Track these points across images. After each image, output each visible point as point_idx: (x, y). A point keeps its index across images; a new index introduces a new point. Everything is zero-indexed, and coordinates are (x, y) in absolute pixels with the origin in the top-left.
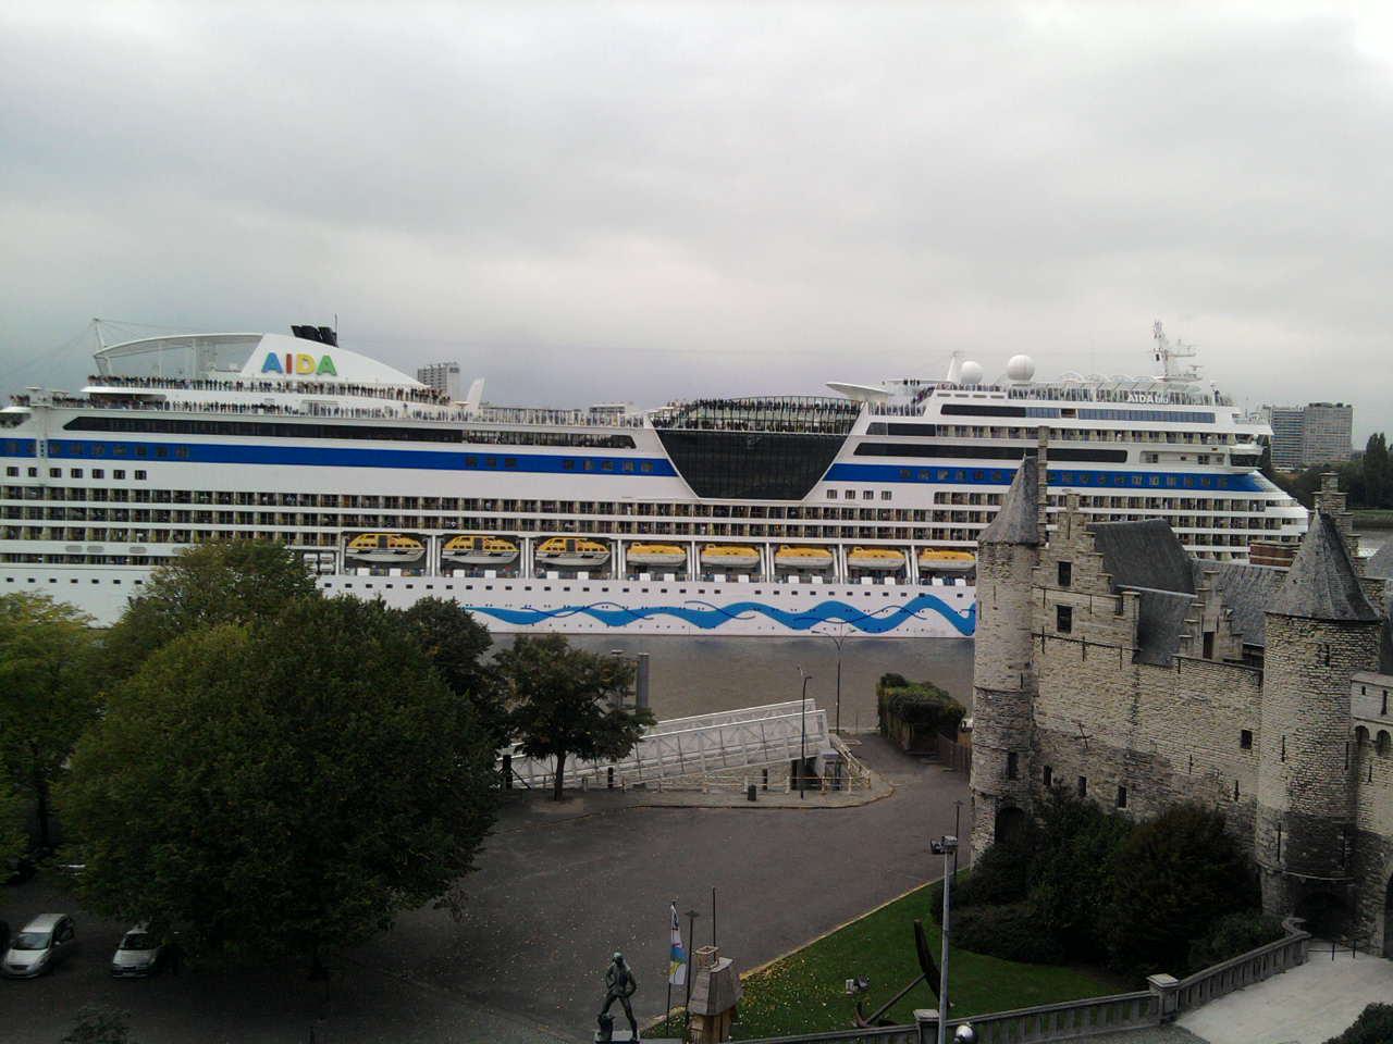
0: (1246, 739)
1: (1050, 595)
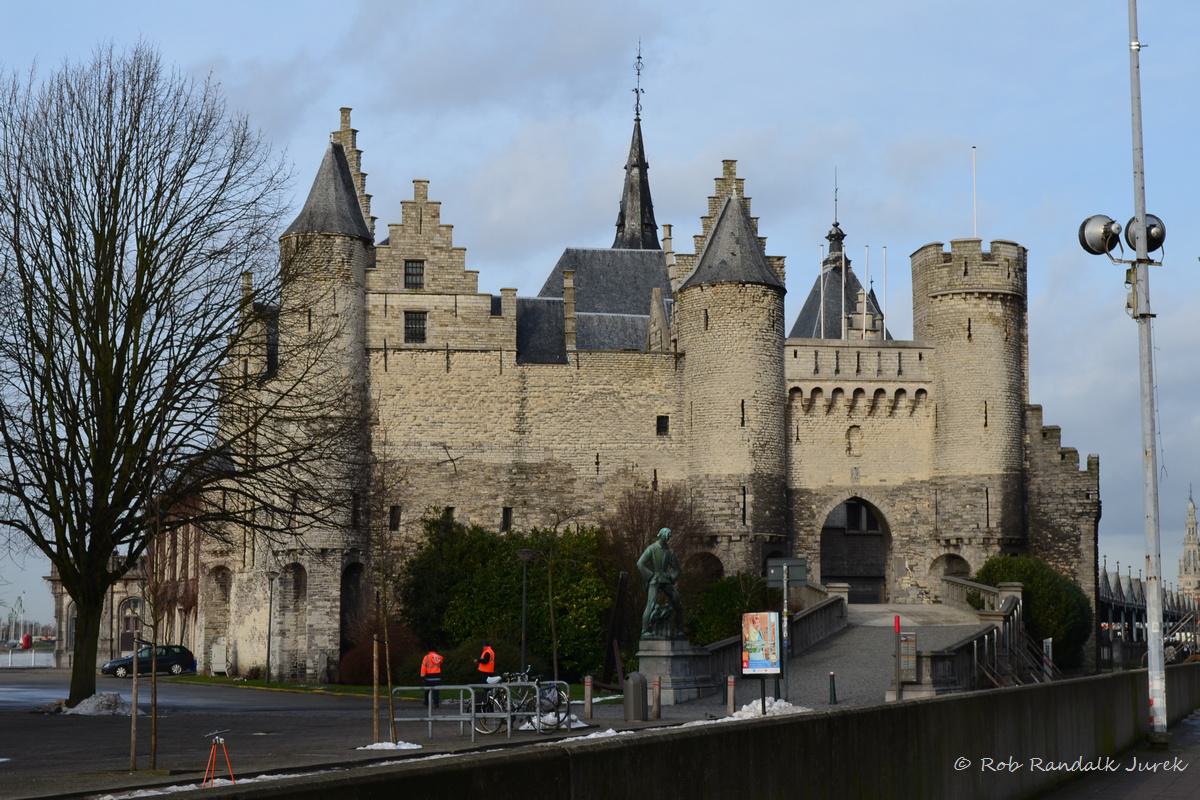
0: (662, 425)
1: (393, 300)
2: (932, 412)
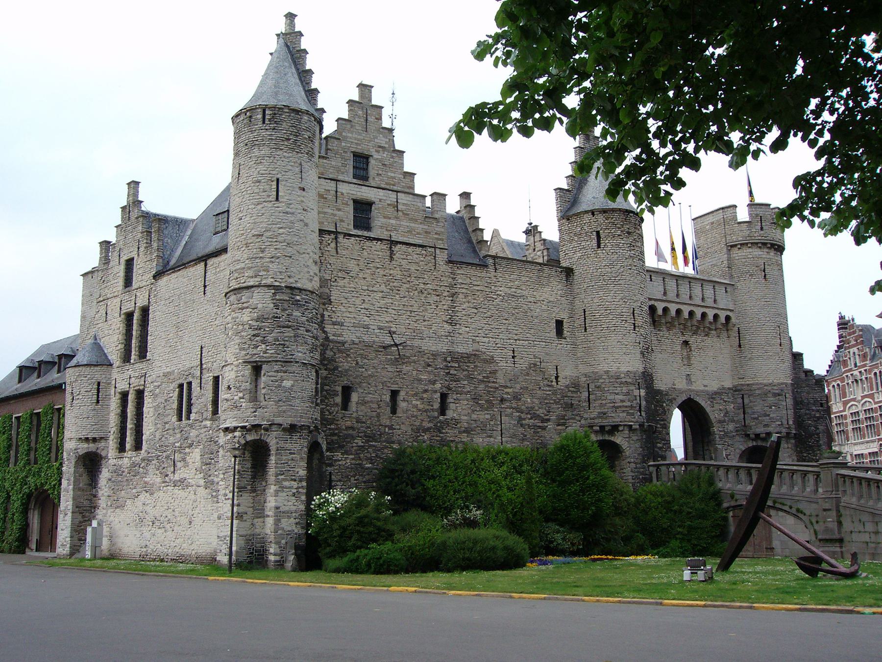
1: (343, 188)
2: (734, 333)
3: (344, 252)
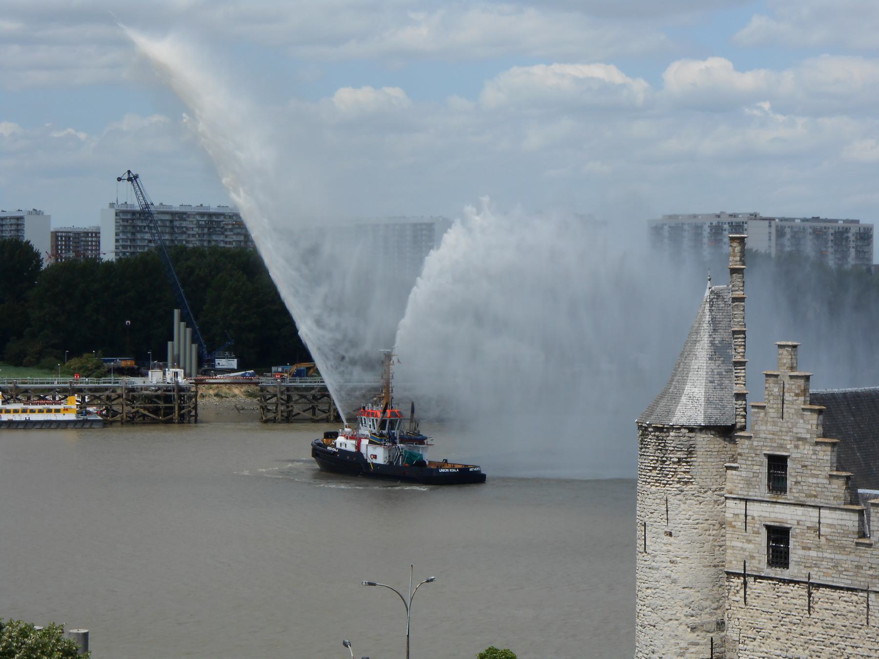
1: (755, 509)
3: (755, 602)
